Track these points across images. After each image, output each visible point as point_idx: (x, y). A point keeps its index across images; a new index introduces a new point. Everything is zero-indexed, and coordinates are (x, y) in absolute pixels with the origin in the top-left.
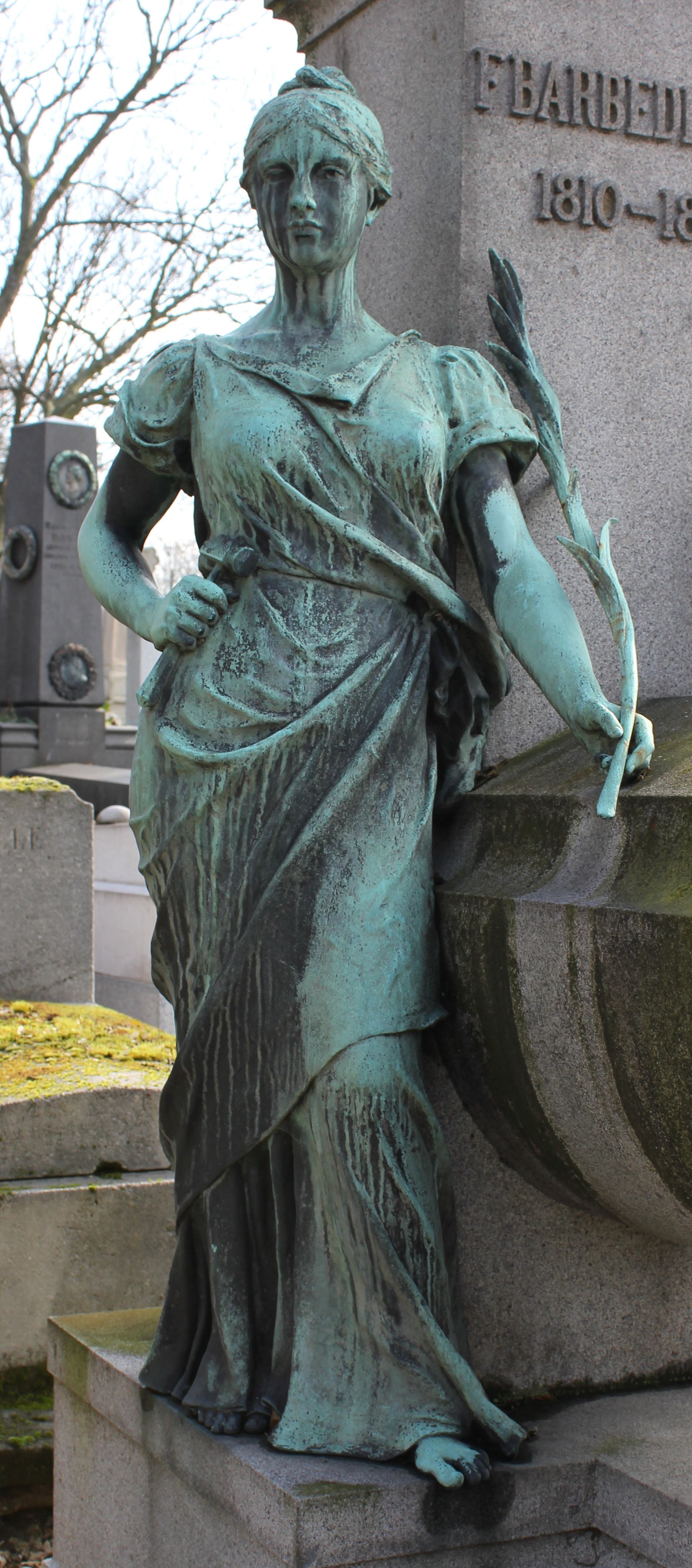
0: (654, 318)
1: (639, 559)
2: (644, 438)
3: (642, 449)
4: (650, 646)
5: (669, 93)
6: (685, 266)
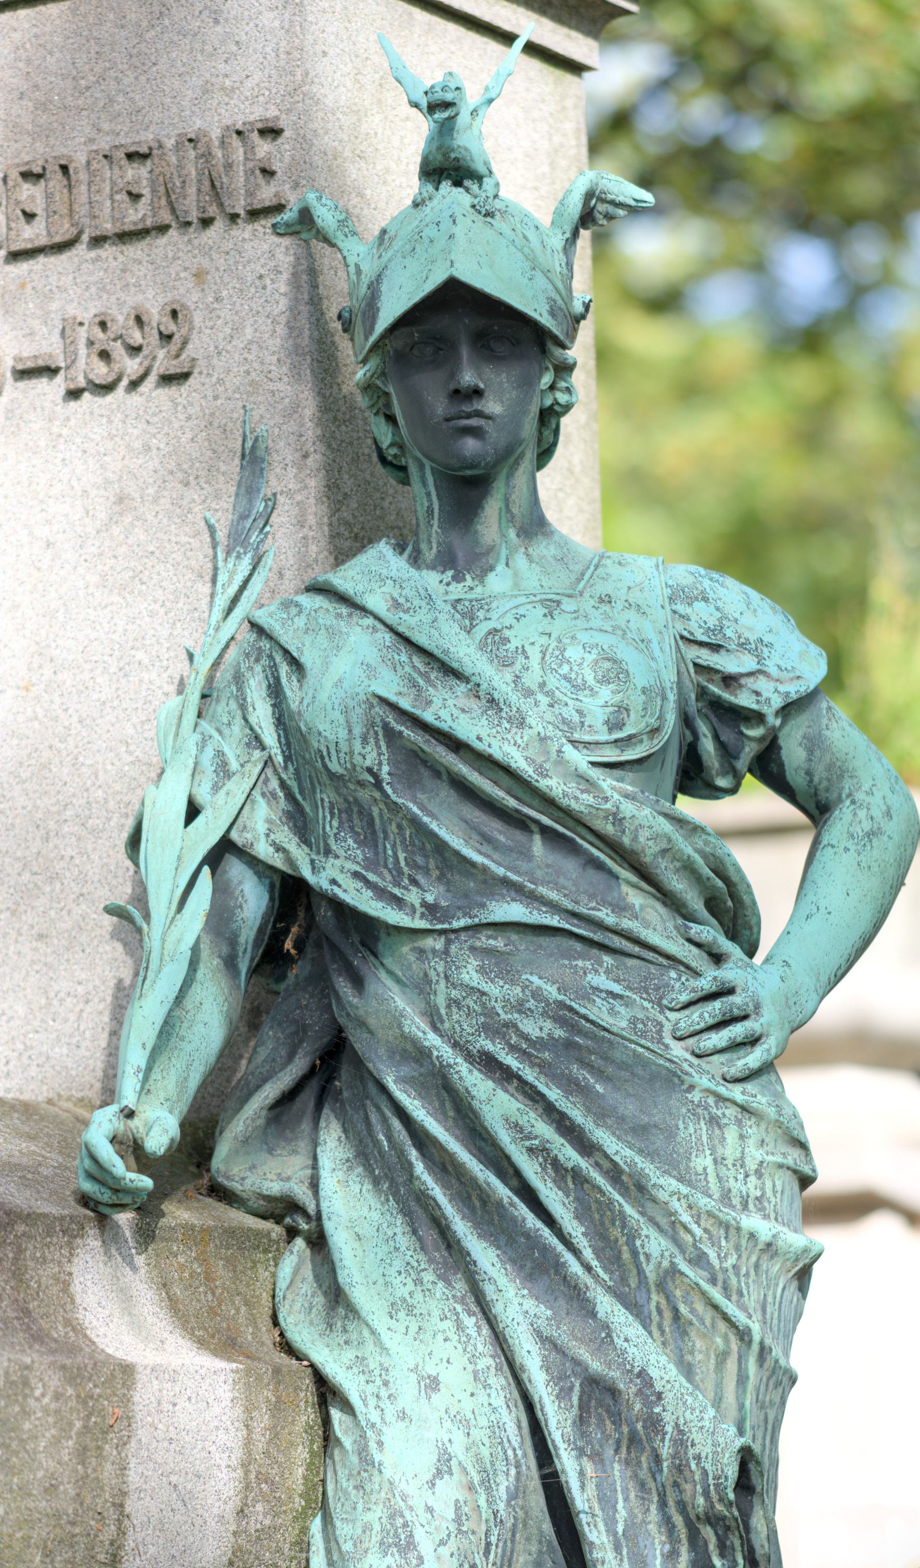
0: (66, 515)
1: (58, 886)
2: (58, 700)
3: (56, 719)
4: (79, 1018)
5: (64, 169)
6: (110, 422)
